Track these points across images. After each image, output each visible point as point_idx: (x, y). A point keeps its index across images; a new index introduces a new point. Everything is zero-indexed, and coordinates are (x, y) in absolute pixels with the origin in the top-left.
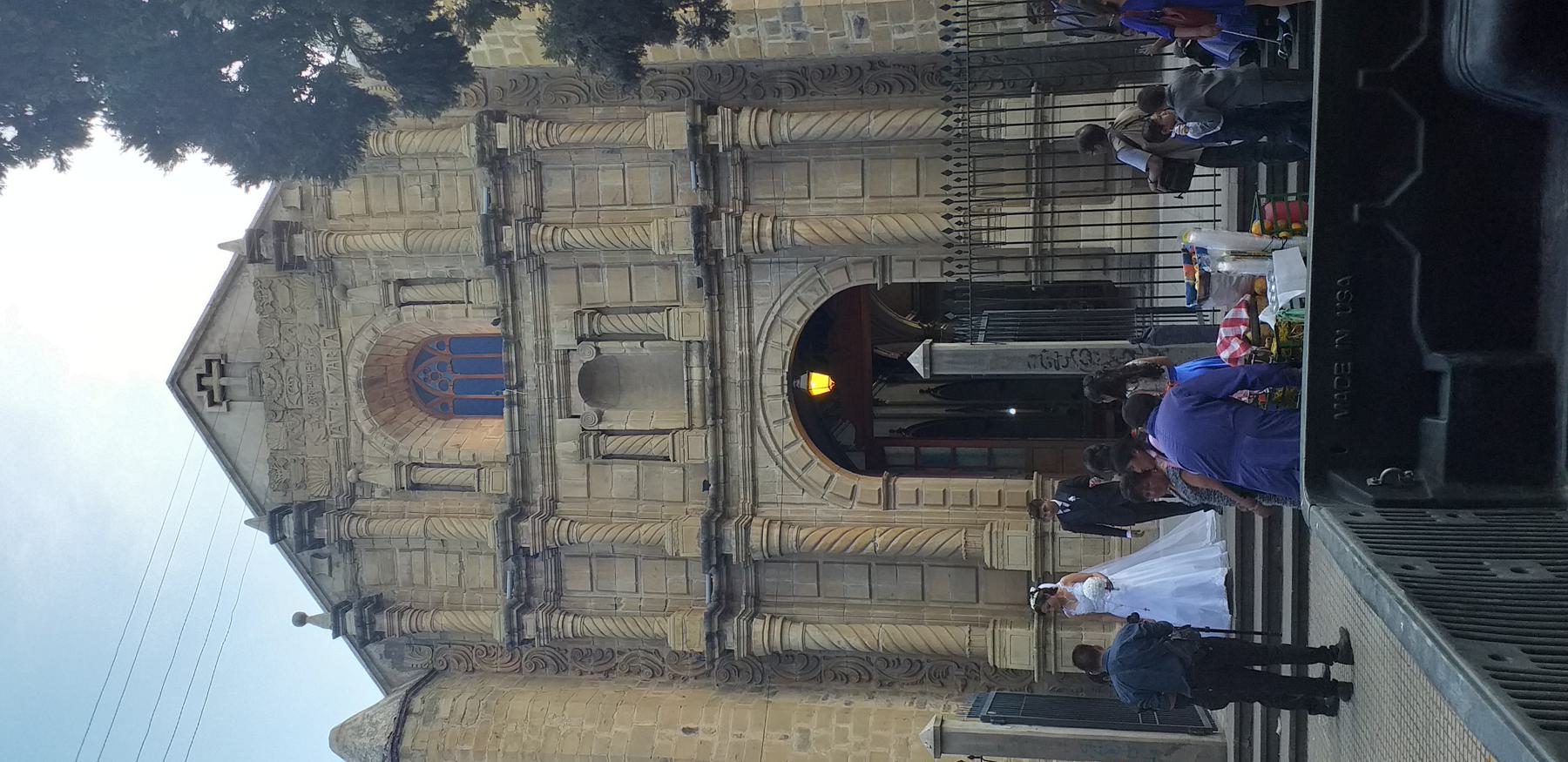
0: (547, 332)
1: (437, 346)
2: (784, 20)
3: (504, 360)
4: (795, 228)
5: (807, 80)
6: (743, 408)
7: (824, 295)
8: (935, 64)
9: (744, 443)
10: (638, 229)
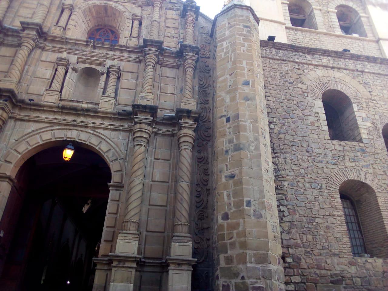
0: (114, 59)
1: (115, 37)
2: (234, 145)
3: (105, 43)
4: (142, 147)
5: (204, 163)
6: (64, 120)
7: (110, 160)
8: (207, 217)
9: (47, 118)
10: (150, 91)
